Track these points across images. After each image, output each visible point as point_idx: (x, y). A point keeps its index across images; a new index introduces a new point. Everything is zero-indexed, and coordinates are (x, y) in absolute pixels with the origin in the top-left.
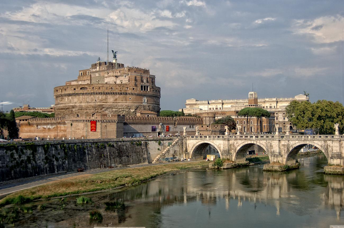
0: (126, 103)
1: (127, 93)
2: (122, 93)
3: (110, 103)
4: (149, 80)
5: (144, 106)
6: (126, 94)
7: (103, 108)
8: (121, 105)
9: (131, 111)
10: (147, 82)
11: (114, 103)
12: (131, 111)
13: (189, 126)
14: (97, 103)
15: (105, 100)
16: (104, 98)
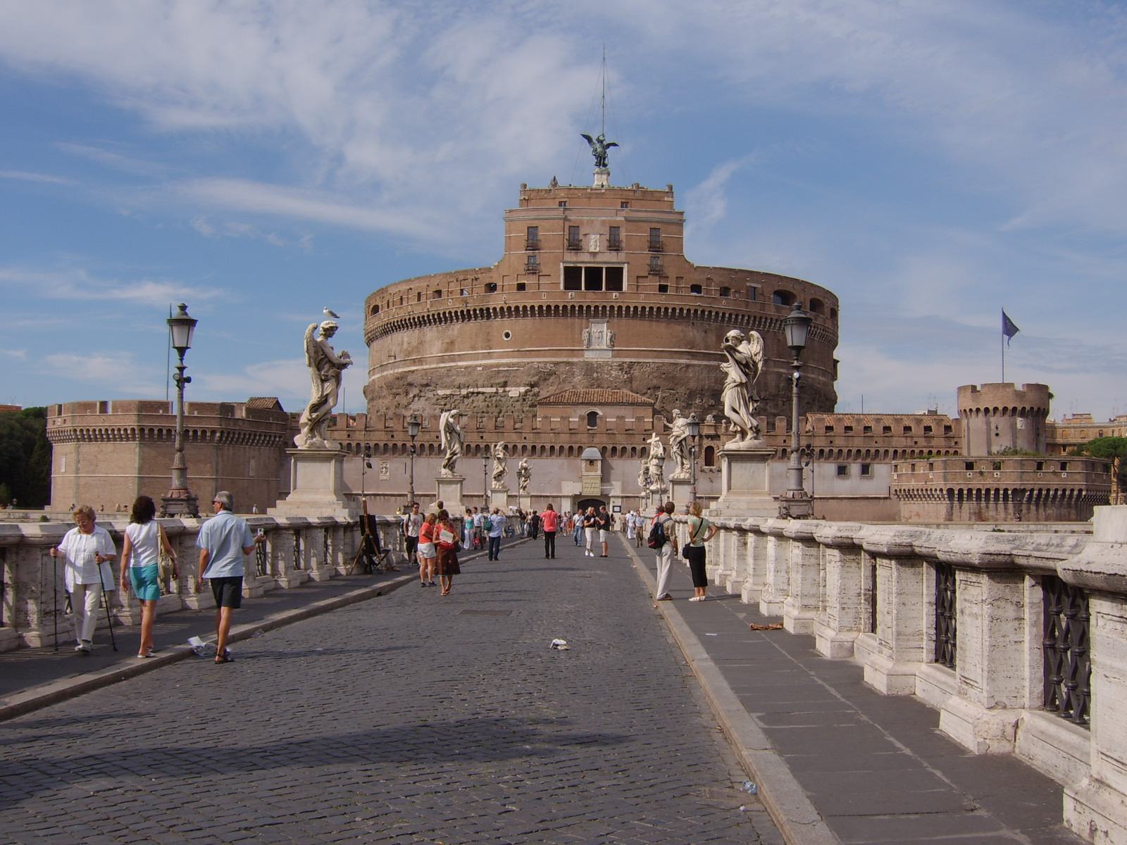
0: (489, 356)
1: (488, 309)
2: (468, 311)
3: (431, 363)
4: (623, 234)
5: (589, 368)
6: (486, 314)
7: (410, 385)
8: (466, 368)
9: (510, 394)
10: (614, 245)
11: (442, 359)
12: (510, 394)
13: (830, 468)
14: (398, 368)
15: (418, 352)
16: (415, 344)
